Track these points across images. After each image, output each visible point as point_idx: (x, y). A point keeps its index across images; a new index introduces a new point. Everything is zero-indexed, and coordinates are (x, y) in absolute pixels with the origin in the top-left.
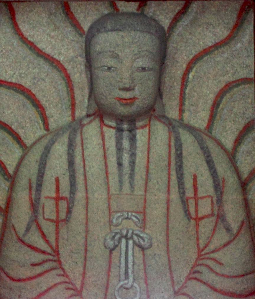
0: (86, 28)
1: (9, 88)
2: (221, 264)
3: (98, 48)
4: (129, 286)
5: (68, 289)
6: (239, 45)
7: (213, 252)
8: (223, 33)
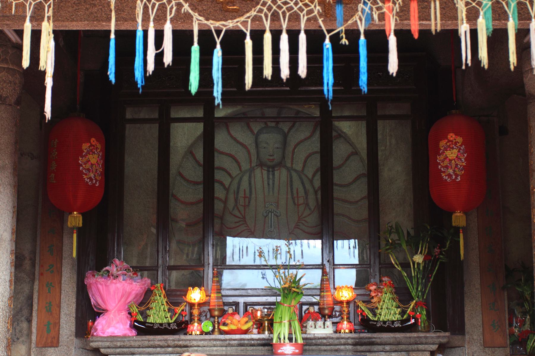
0: (256, 132)
1: (226, 155)
2: (307, 222)
3: (260, 140)
4: (272, 230)
5: (248, 232)
6: (314, 139)
7: (304, 218)
8: (308, 134)
